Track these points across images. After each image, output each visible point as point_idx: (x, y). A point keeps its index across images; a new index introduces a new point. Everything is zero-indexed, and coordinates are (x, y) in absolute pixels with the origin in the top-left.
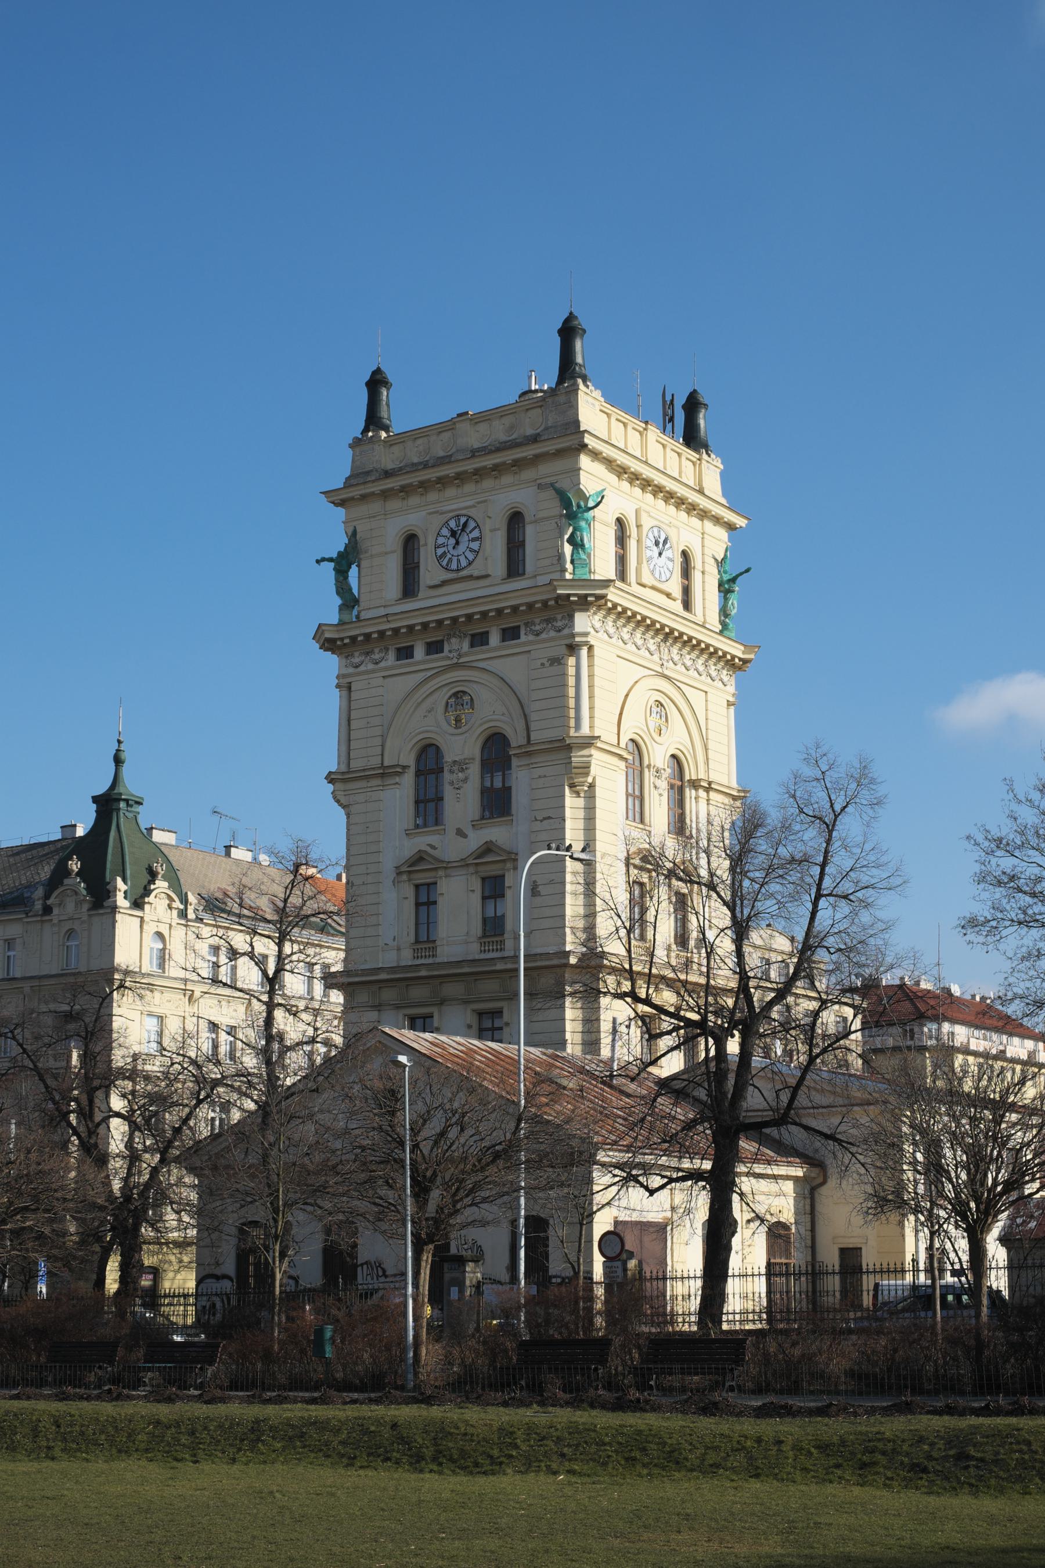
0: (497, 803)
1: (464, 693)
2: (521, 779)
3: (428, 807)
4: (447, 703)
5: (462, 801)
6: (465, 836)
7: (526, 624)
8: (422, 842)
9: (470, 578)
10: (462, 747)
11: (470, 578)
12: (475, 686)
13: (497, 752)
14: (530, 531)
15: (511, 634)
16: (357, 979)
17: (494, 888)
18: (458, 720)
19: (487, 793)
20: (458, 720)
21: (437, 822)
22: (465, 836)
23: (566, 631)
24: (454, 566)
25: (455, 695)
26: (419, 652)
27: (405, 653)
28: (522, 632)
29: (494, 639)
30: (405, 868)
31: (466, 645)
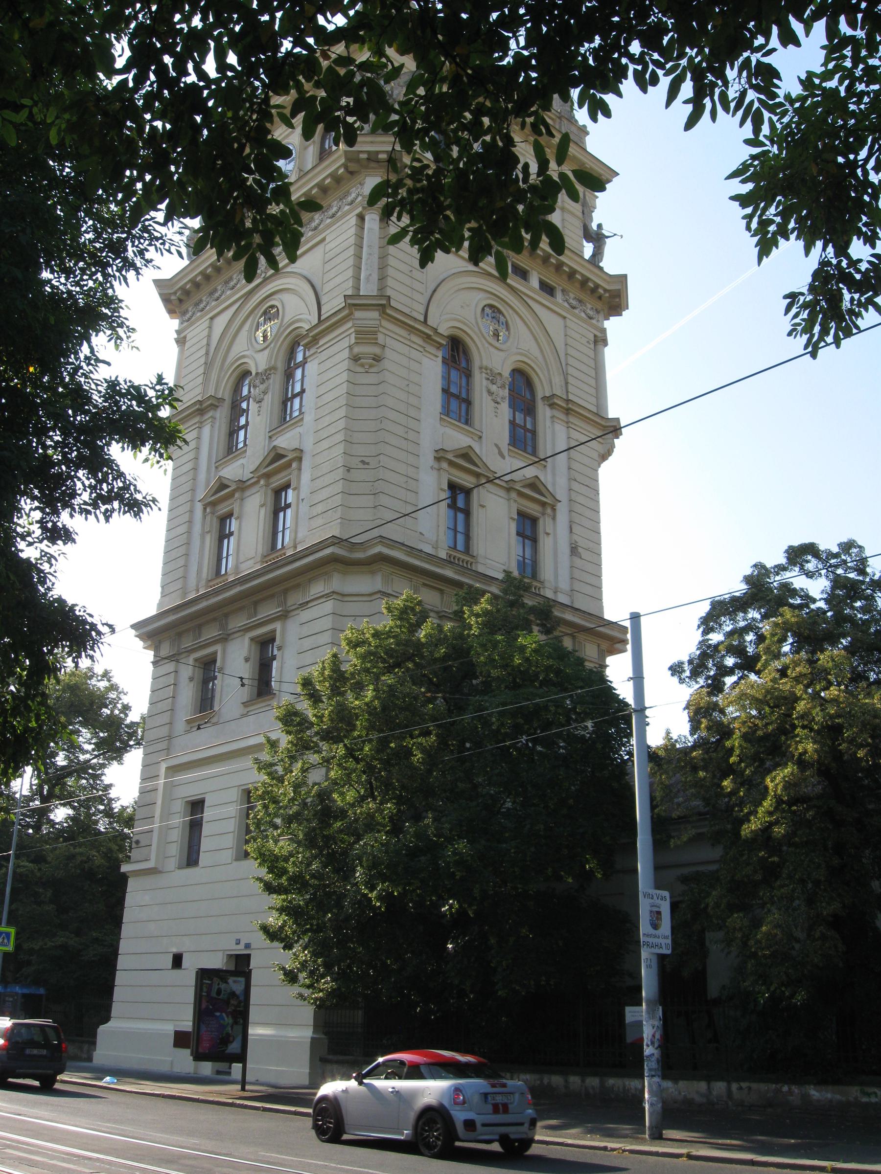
0: (523, 439)
1: (500, 312)
2: (554, 433)
3: (458, 403)
4: (483, 309)
5: (494, 417)
7: (563, 291)
8: (457, 439)
12: (511, 311)
13: (522, 389)
15: (547, 288)
16: (417, 563)
17: (528, 528)
20: (496, 335)
22: (503, 457)
23: (594, 321)
25: (491, 306)
28: (559, 296)
30: (450, 456)
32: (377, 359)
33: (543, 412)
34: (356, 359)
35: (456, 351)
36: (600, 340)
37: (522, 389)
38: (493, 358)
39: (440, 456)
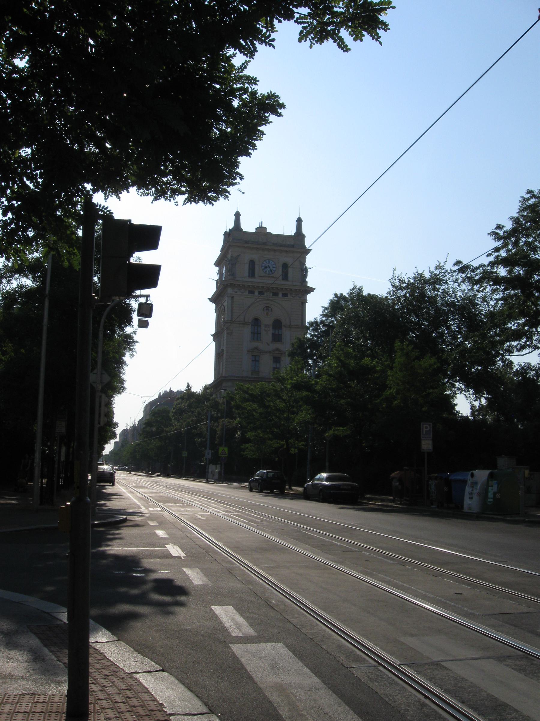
3: (256, 335)
5: (267, 335)
6: (268, 345)
9: (273, 277)
10: (267, 320)
11: (273, 277)
13: (277, 324)
14: (290, 270)
15: (285, 295)
18: (267, 314)
19: (274, 335)
20: (267, 314)
21: (260, 340)
22: (268, 345)
24: (268, 273)
25: (266, 307)
26: (256, 293)
27: (252, 292)
28: (289, 295)
29: (280, 295)
31: (271, 294)
32: (232, 333)
33: (284, 329)
34: (228, 333)
35: (256, 322)
36: (304, 302)
37: (277, 324)
38: (267, 320)
39: (248, 351)
